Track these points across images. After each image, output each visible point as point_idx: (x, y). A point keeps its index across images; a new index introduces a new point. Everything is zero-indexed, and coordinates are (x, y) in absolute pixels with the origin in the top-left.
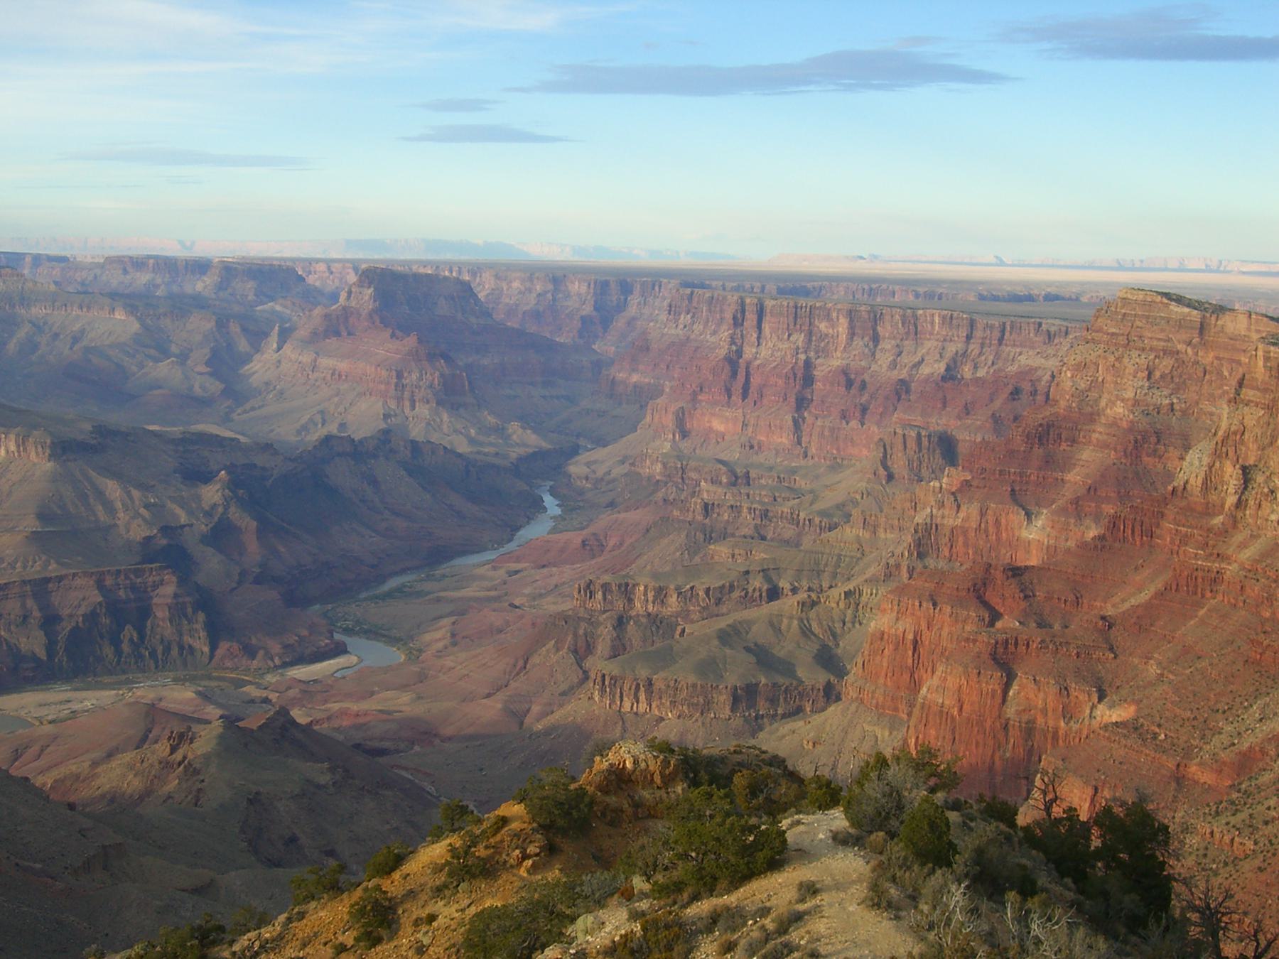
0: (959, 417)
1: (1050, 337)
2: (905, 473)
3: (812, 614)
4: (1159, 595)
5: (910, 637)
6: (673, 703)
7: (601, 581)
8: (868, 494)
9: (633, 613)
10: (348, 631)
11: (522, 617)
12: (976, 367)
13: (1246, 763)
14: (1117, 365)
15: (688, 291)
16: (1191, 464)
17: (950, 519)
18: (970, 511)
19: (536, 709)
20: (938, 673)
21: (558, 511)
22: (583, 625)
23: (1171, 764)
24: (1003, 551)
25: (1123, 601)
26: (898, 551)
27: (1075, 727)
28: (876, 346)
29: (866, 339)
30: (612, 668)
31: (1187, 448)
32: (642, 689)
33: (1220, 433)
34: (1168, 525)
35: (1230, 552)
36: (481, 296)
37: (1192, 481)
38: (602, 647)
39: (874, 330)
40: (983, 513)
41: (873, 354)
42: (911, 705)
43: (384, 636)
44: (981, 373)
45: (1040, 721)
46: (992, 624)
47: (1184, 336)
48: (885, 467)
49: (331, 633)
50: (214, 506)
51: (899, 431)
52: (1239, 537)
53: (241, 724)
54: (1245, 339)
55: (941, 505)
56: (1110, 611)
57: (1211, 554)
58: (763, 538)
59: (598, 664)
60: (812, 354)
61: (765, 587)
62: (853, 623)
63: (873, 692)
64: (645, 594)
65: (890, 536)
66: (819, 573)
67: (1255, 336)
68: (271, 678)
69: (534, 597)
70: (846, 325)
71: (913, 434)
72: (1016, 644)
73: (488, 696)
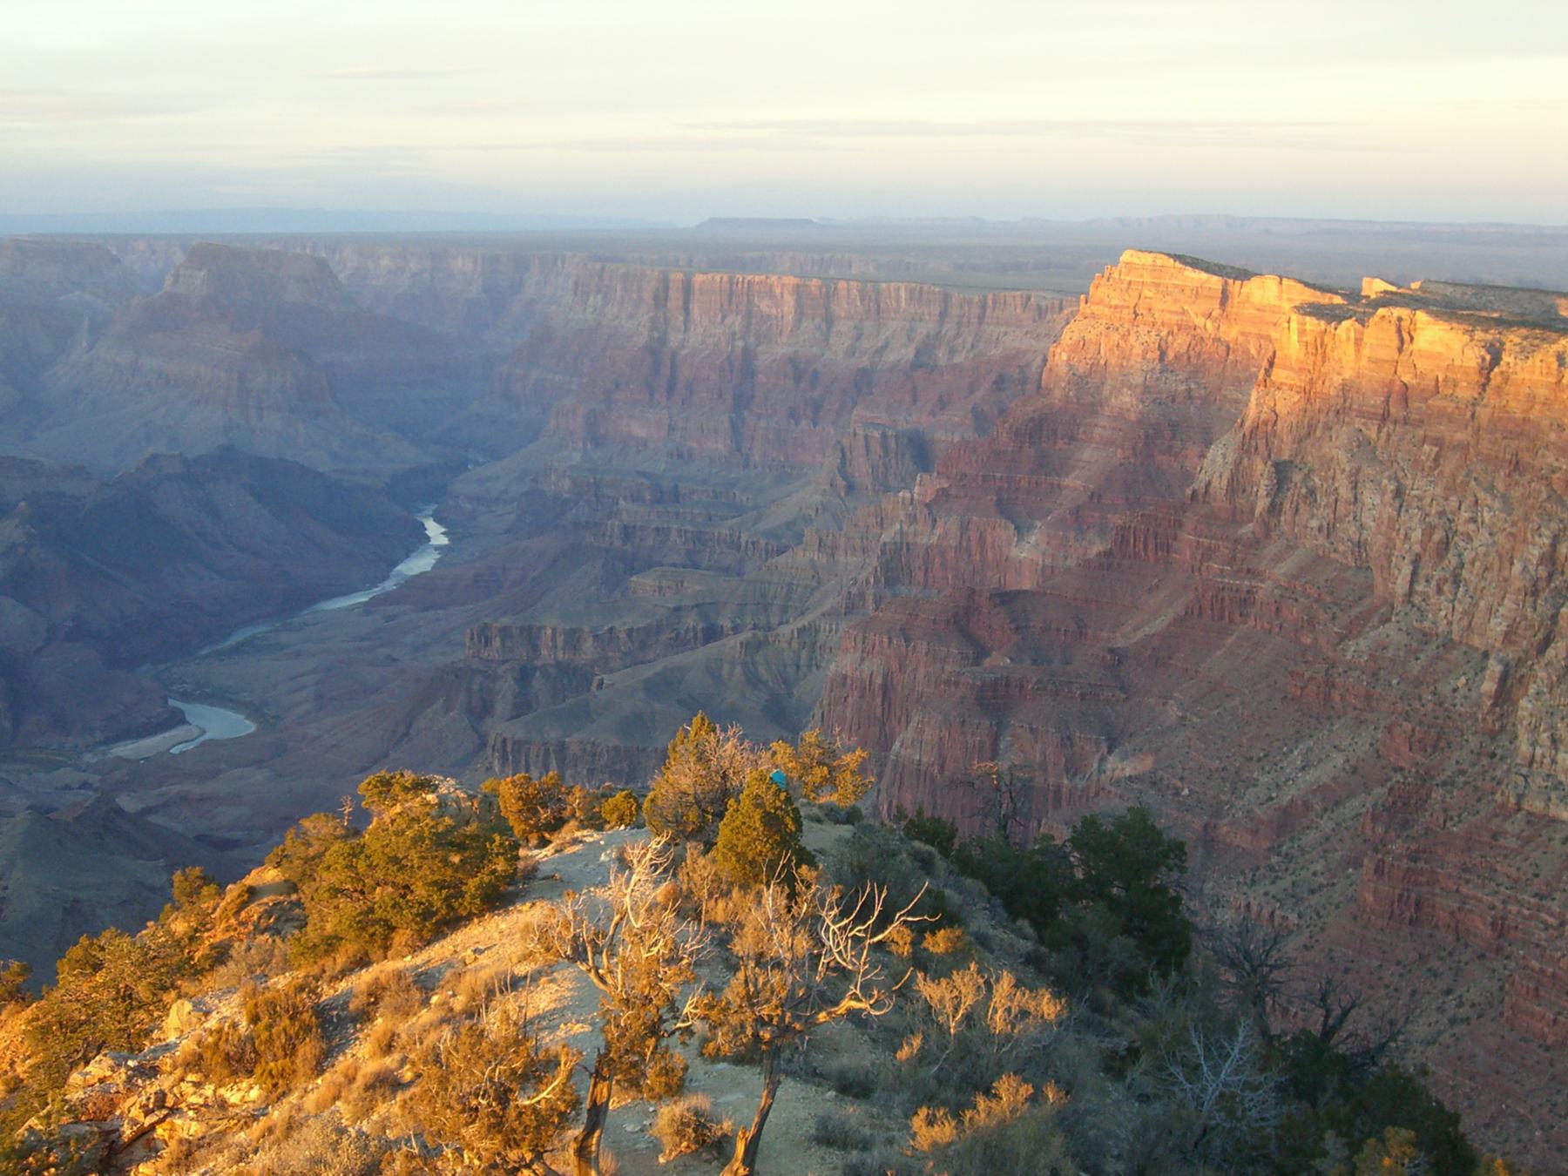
0: (933, 413)
1: (1041, 313)
2: (868, 482)
3: (759, 658)
4: (1179, 621)
5: (879, 681)
6: (591, 772)
7: (498, 625)
8: (825, 509)
9: (538, 663)
10: (186, 696)
12: (952, 352)
13: (1288, 820)
14: (1122, 344)
15: (598, 266)
16: (1213, 461)
17: (925, 537)
18: (948, 527)
20: (913, 724)
21: (445, 541)
22: (478, 679)
23: (1198, 824)
24: (990, 574)
25: (1136, 629)
26: (862, 578)
27: (1081, 784)
28: (829, 329)
29: (818, 320)
30: (515, 731)
31: (1208, 443)
32: (553, 755)
33: (1248, 423)
34: (1187, 537)
35: (1262, 567)
36: (341, 277)
37: (1215, 483)
38: (502, 706)
39: (827, 308)
40: (964, 528)
41: (827, 340)
42: (882, 764)
44: (958, 359)
45: (1039, 779)
46: (977, 662)
47: (1203, 306)
48: (845, 476)
49: (165, 698)
50: (13, 546)
51: (860, 431)
52: (1271, 549)
53: (52, 816)
54: (1275, 310)
55: (913, 519)
56: (1120, 643)
57: (1239, 571)
58: (697, 566)
59: (500, 728)
60: (752, 340)
61: (701, 626)
62: (810, 671)
64: (554, 638)
65: (852, 559)
66: (766, 607)
67: (1287, 306)
68: (89, 758)
70: (792, 303)
71: (877, 434)
72: (1007, 685)
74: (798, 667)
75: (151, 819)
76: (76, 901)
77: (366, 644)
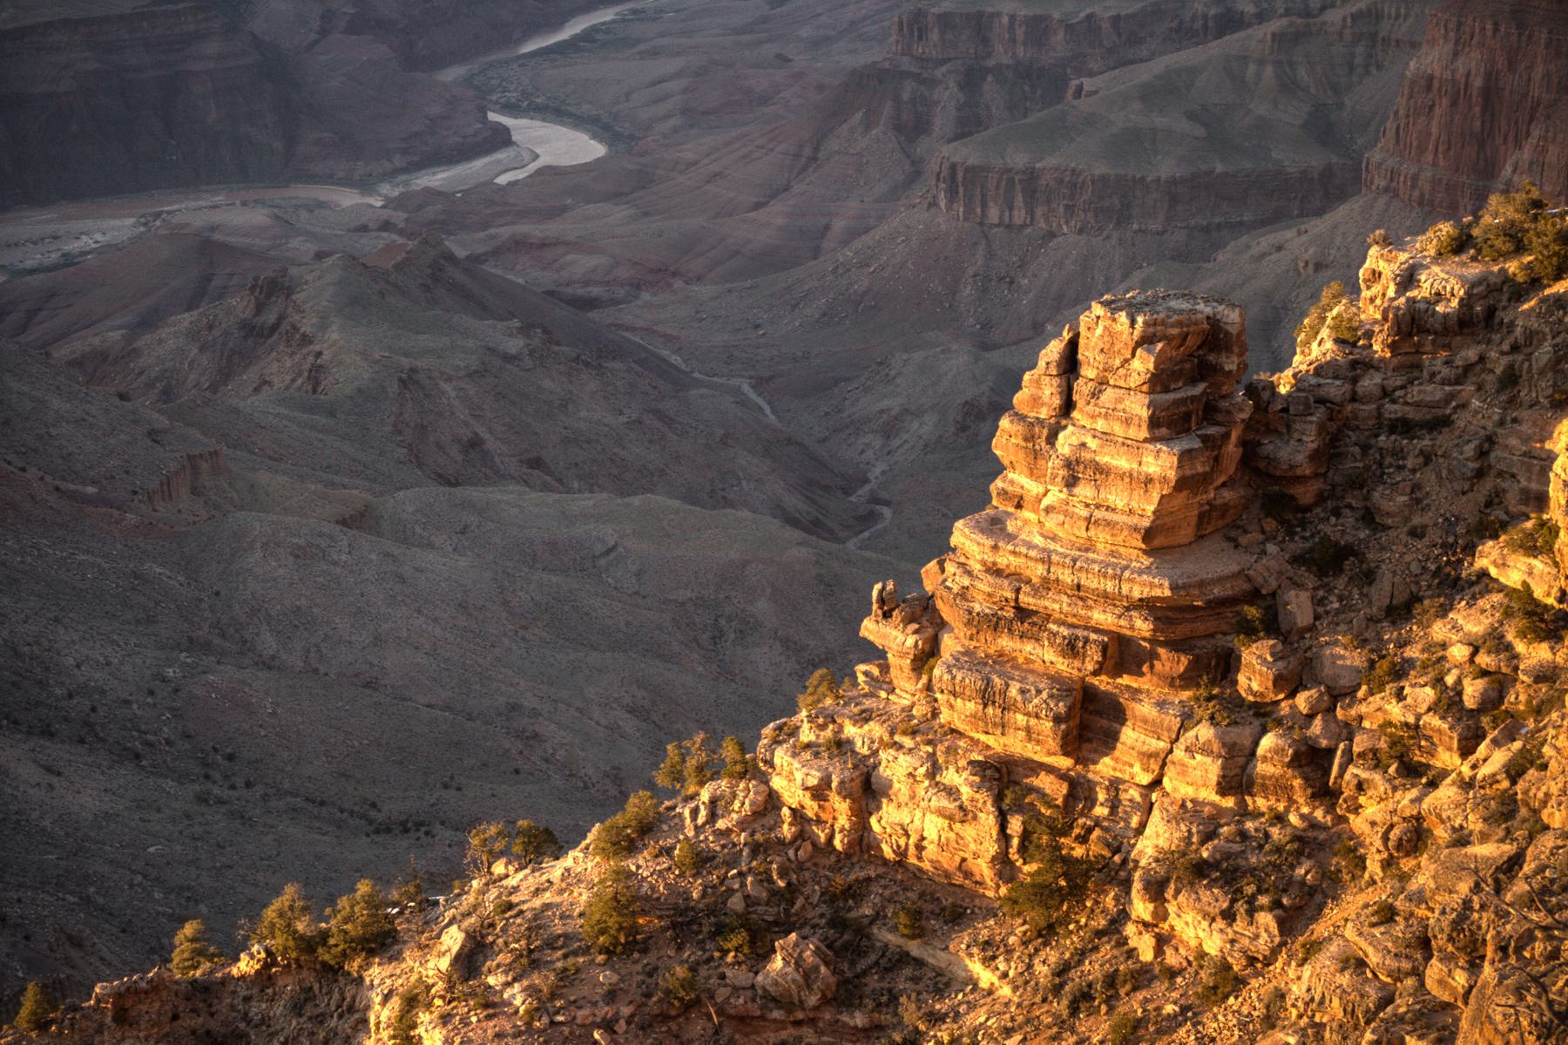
5: (1478, 83)
6: (1070, 210)
7: (936, 10)
10: (511, 109)
11: (799, 76)
19: (839, 225)
32: (1018, 187)
43: (571, 115)
49: (483, 111)
61: (1212, 12)
62: (1368, 72)
63: (1415, 178)
69: (816, 43)
73: (757, 206)
74: (1351, 68)
75: (489, 268)
76: (413, 370)
77: (746, 38)
